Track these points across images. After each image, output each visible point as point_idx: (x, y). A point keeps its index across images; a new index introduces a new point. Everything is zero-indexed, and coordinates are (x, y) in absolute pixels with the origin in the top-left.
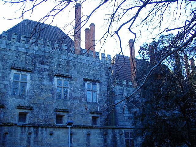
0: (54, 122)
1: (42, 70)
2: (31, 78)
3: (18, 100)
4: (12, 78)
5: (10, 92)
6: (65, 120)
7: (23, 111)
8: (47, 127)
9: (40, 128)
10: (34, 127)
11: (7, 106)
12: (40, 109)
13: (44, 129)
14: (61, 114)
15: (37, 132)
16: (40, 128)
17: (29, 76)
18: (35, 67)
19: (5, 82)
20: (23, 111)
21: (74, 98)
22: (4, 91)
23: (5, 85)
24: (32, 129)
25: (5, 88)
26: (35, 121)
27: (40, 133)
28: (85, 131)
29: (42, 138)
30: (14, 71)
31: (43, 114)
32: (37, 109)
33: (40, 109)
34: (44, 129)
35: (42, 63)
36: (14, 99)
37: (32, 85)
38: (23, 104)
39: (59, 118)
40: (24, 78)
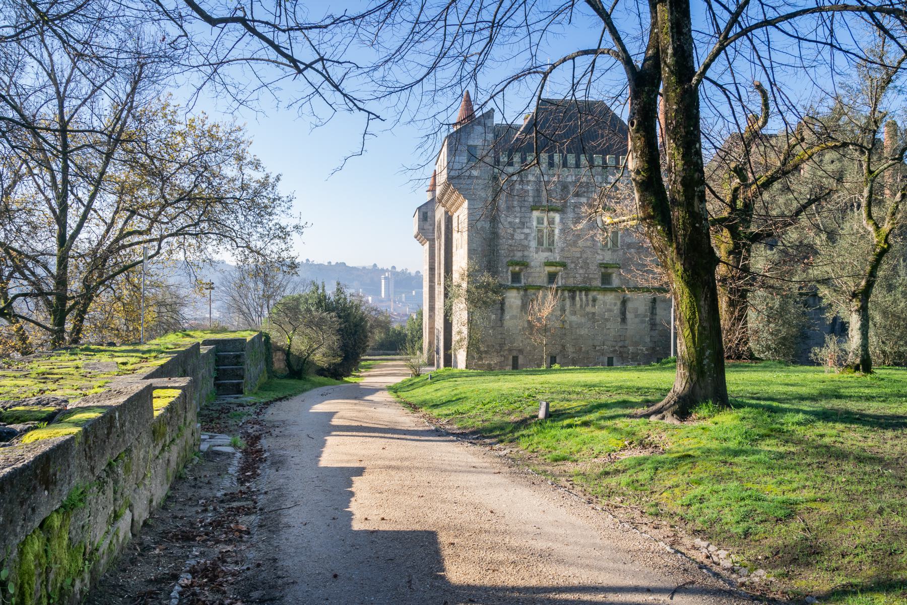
0: (597, 283)
1: (575, 206)
2: (562, 219)
3: (546, 254)
4: (535, 223)
5: (533, 244)
6: (616, 282)
7: (552, 269)
8: (587, 290)
9: (578, 293)
10: (569, 291)
11: (532, 264)
12: (576, 265)
13: (584, 293)
14: (610, 271)
15: (573, 298)
16: (578, 293)
17: (557, 217)
18: (566, 202)
19: (526, 231)
20: (552, 269)
21: (629, 246)
22: (526, 243)
23: (527, 235)
24: (566, 294)
25: (526, 238)
26: (571, 282)
27: (577, 298)
28: (648, 296)
29: (581, 306)
30: (536, 214)
31: (581, 271)
32: (573, 266)
33: (576, 265)
34: (584, 293)
35: (577, 195)
36: (540, 253)
37: (563, 231)
38: (551, 259)
39: (606, 278)
40: (551, 222)
